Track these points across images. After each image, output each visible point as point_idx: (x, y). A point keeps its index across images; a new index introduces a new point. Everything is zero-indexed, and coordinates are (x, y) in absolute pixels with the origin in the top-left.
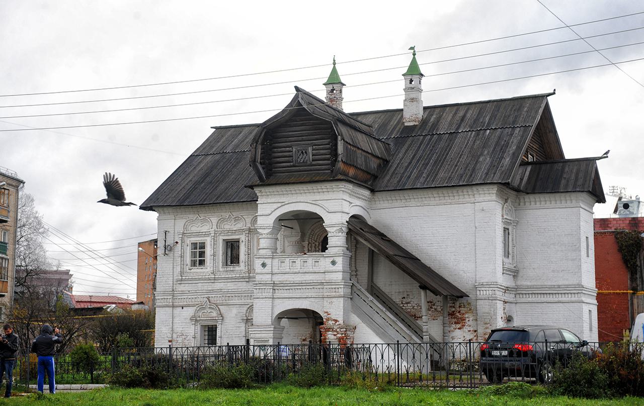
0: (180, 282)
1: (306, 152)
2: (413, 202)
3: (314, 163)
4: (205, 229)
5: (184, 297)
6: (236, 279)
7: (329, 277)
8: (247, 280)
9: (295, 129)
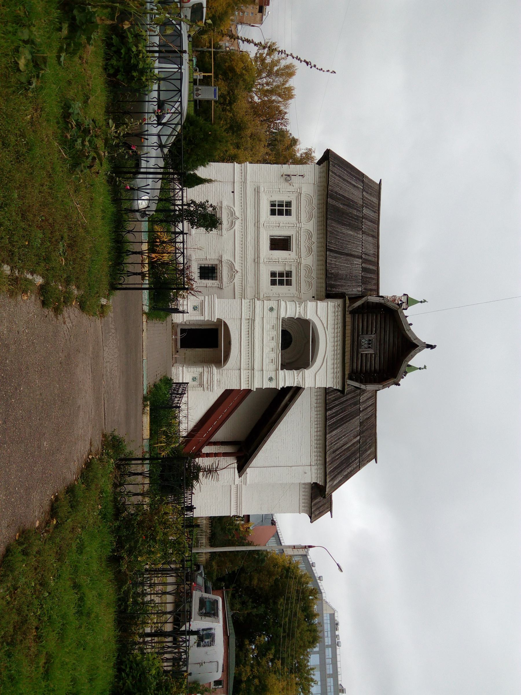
0: (256, 190)
1: (369, 347)
2: (314, 413)
3: (360, 355)
4: (304, 216)
5: (243, 194)
6: (257, 250)
7: (257, 374)
8: (256, 261)
9: (392, 336)
